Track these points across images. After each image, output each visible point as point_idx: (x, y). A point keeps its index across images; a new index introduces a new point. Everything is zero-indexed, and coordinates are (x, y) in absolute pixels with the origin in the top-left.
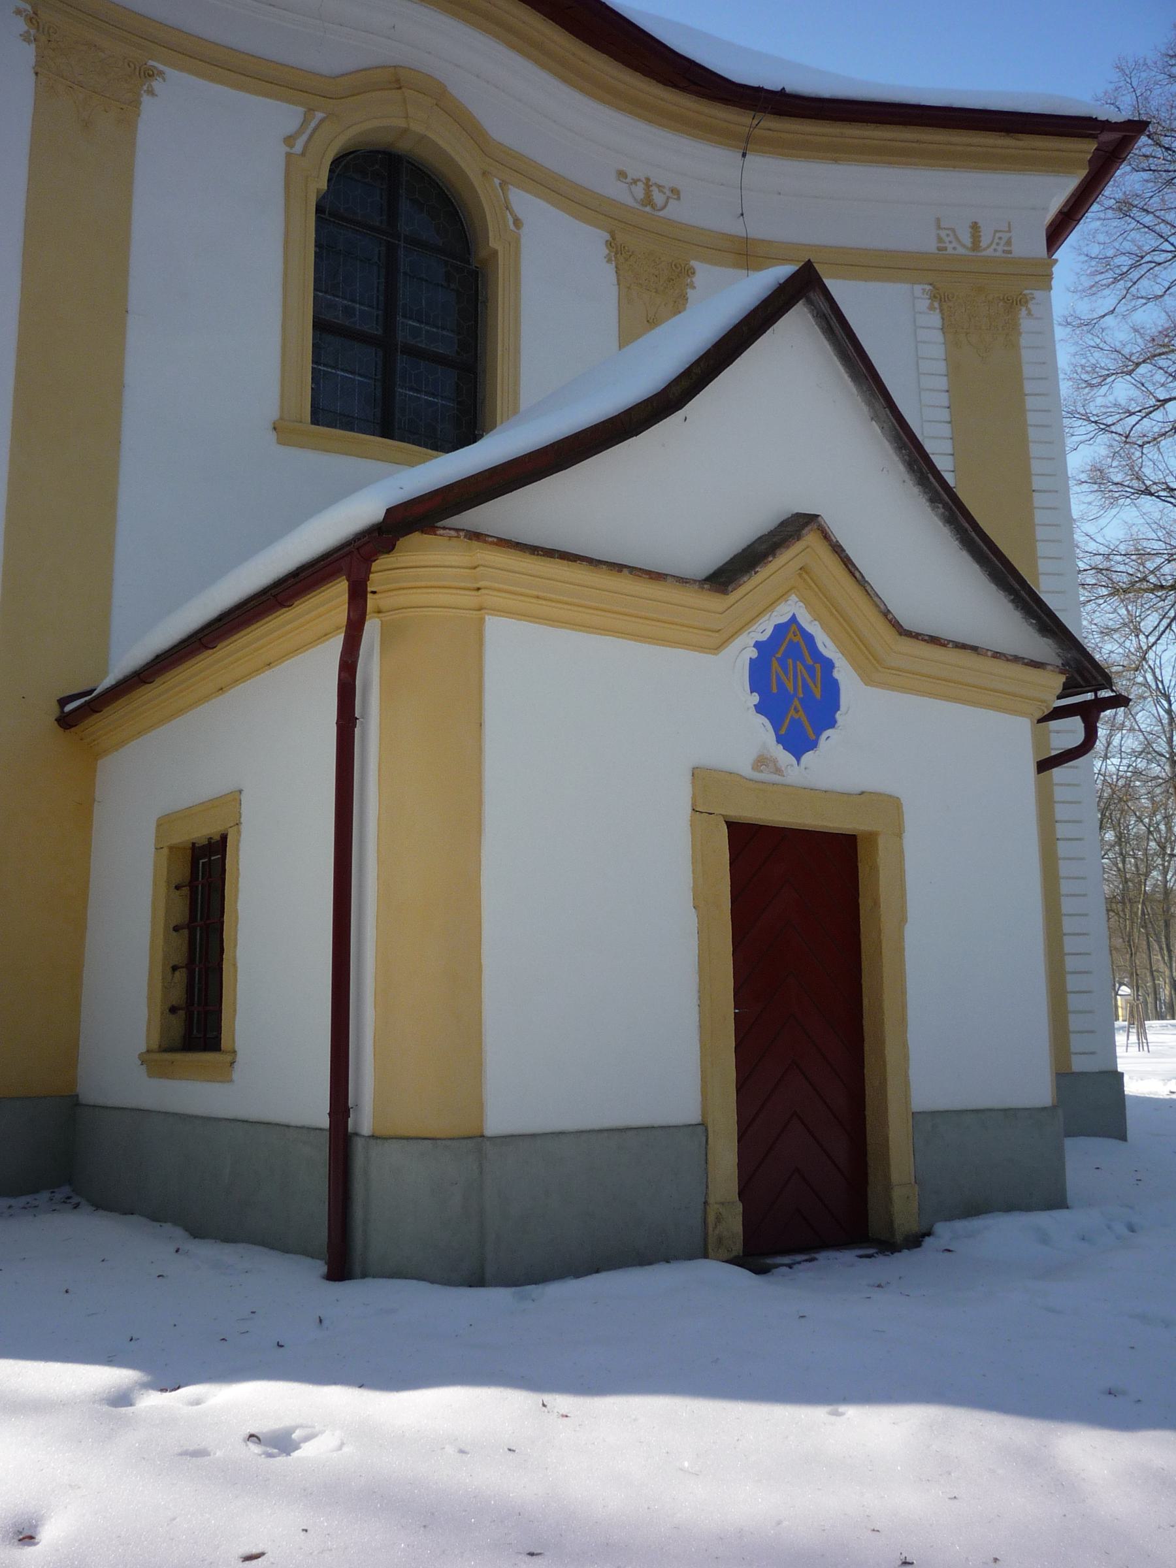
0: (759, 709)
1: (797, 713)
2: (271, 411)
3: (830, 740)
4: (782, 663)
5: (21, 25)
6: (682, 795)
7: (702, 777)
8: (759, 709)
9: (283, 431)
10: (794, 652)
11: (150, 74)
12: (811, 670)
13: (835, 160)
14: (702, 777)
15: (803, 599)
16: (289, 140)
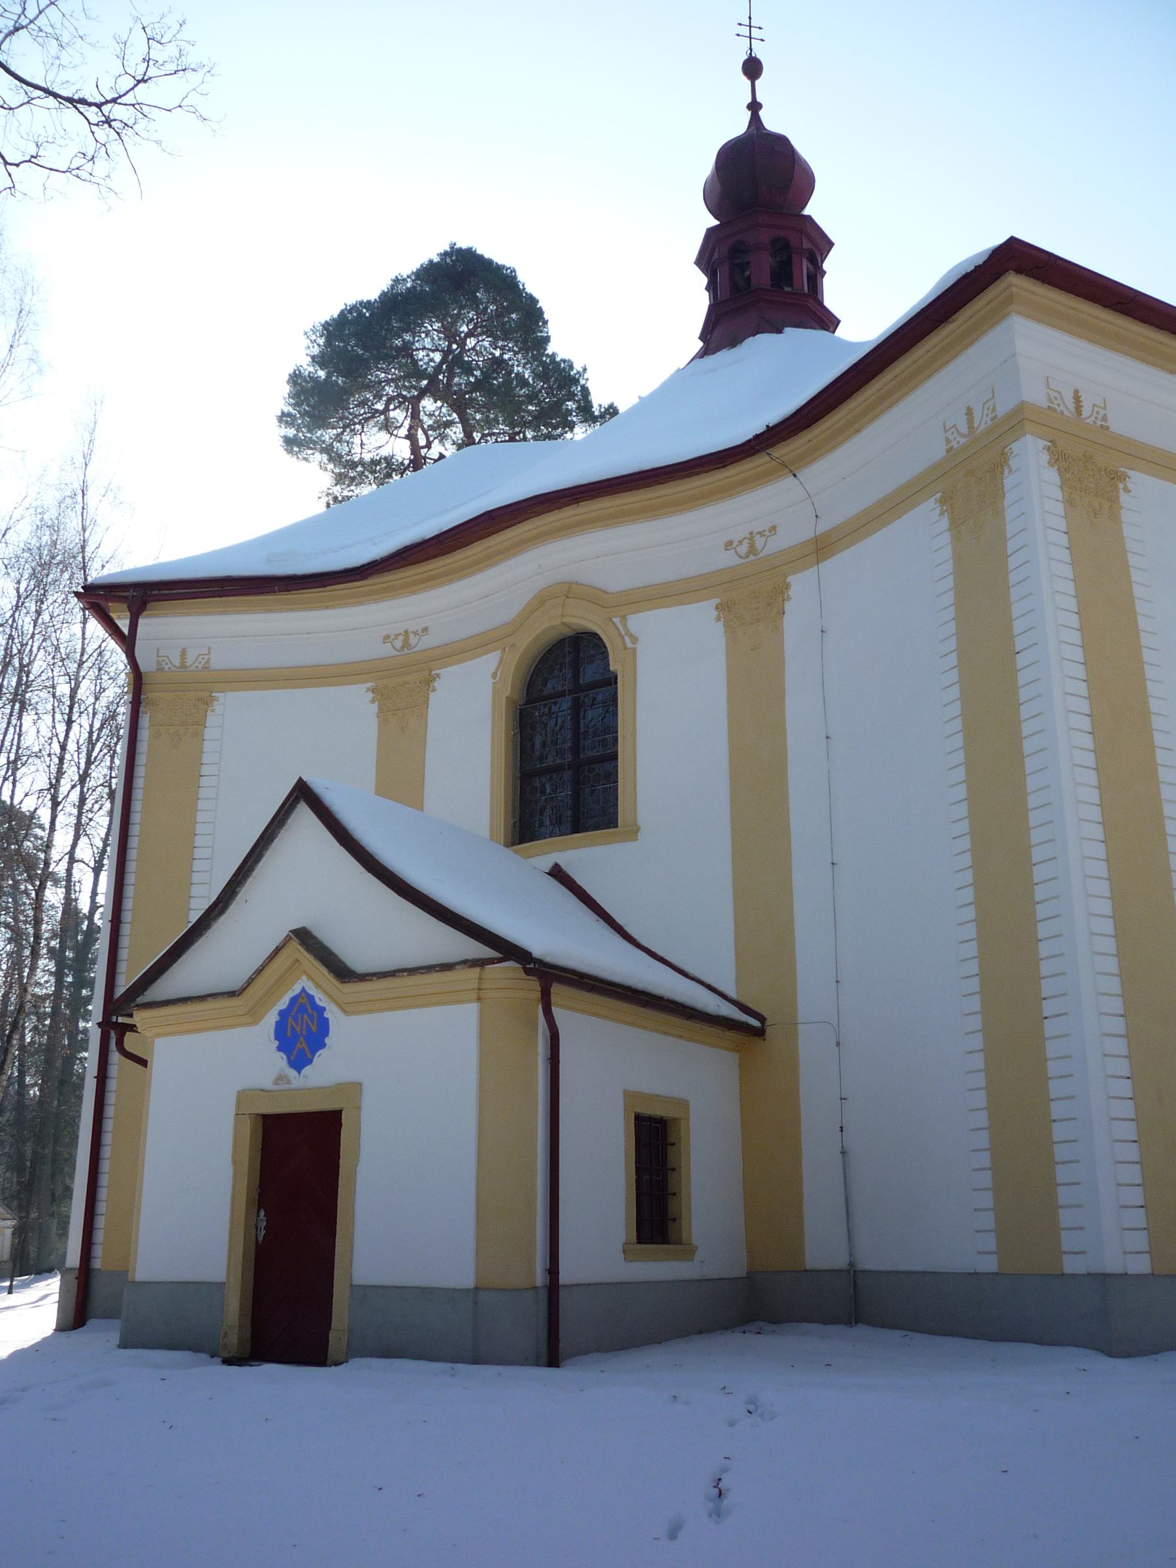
0: (279, 1049)
1: (302, 1044)
4: (295, 1019)
5: (370, 695)
8: (279, 1049)
10: (303, 1009)
12: (311, 1017)
13: (859, 431)
15: (310, 978)
16: (494, 675)
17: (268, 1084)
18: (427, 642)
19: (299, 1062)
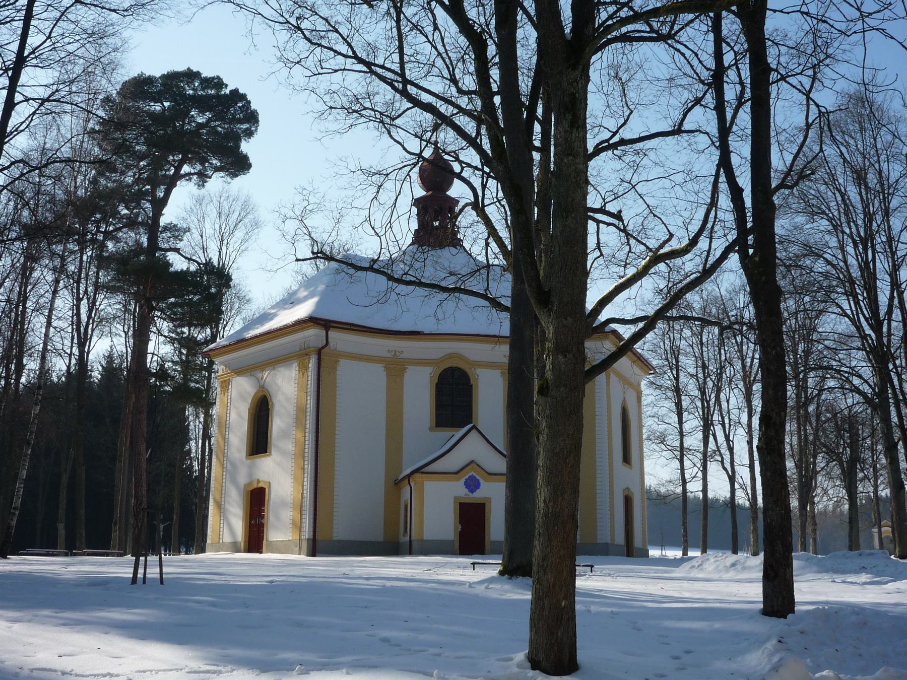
2: (428, 426)
3: (478, 491)
6: (452, 500)
7: (456, 498)
9: (431, 429)
11: (405, 369)
14: (456, 498)
17: (463, 496)
18: (402, 356)
19: (472, 491)
